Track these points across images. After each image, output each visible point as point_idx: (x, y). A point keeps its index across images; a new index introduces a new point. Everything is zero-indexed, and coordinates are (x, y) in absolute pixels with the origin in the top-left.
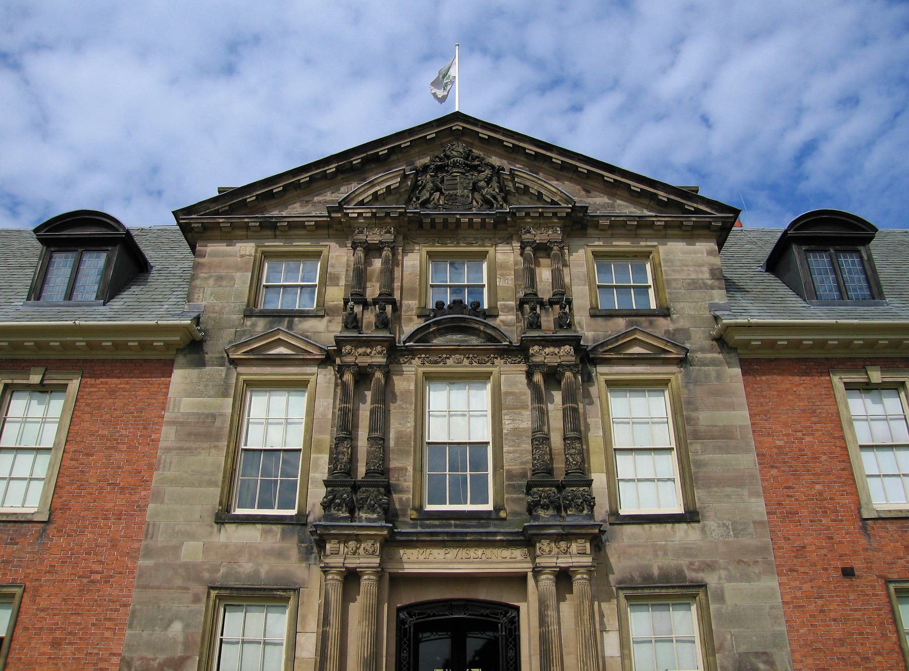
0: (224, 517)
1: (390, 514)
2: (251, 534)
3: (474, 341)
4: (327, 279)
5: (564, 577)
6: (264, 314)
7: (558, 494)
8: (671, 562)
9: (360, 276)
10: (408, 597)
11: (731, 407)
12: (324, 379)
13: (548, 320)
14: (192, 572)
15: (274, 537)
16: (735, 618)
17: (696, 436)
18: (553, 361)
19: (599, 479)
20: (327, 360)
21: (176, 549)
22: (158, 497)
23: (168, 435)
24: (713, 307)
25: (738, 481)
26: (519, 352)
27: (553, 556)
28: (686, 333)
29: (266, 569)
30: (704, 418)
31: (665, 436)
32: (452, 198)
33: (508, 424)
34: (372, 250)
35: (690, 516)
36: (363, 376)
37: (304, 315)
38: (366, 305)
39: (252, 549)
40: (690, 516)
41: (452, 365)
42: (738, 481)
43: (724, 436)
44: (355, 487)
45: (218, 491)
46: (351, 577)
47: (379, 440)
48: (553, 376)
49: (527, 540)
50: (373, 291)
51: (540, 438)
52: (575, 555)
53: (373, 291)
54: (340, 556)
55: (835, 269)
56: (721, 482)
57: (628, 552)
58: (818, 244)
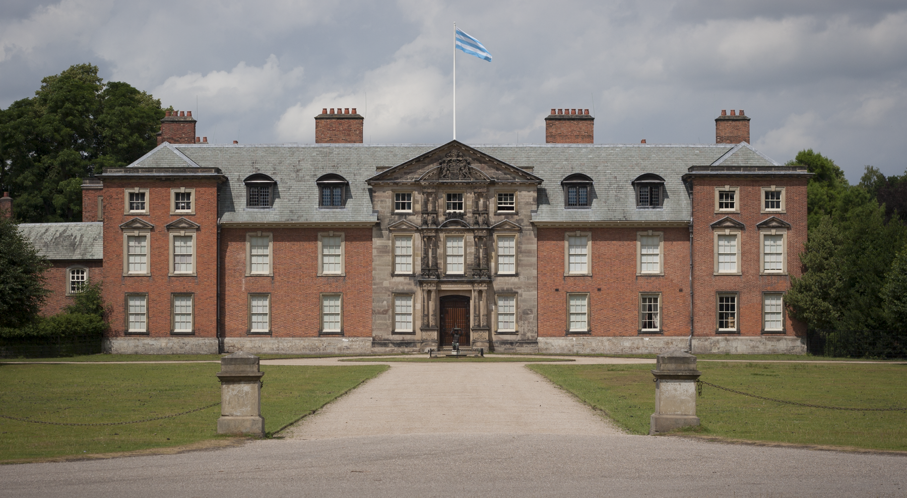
0: (393, 275)
1: (438, 277)
2: (401, 279)
3: (459, 227)
4: (416, 202)
5: (480, 292)
6: (397, 214)
7: (481, 271)
8: (510, 286)
9: (426, 203)
10: (442, 295)
11: (532, 244)
12: (417, 236)
13: (481, 219)
14: (387, 289)
15: (407, 280)
16: (524, 301)
17: (521, 252)
18: (481, 235)
19: (493, 264)
20: (417, 230)
21: (382, 283)
22: (375, 269)
23: (375, 252)
24: (532, 211)
25: (531, 265)
26: (473, 230)
27: (477, 287)
28: (522, 220)
29: (406, 288)
30: (524, 247)
31: (513, 252)
32: (453, 174)
33: (468, 251)
34: (429, 194)
35: (516, 275)
36: (429, 238)
37: (409, 214)
38: (428, 214)
39: (403, 284)
40: (516, 275)
41: (453, 234)
42: (531, 265)
43: (528, 253)
44: (429, 270)
45: (390, 267)
46: (429, 292)
47: (435, 258)
48: (480, 238)
49: (472, 283)
50: (430, 207)
51: (477, 257)
52: (484, 288)
53: (430, 207)
54: (426, 287)
55: (578, 193)
56: (526, 266)
57: (498, 284)
58: (573, 185)
